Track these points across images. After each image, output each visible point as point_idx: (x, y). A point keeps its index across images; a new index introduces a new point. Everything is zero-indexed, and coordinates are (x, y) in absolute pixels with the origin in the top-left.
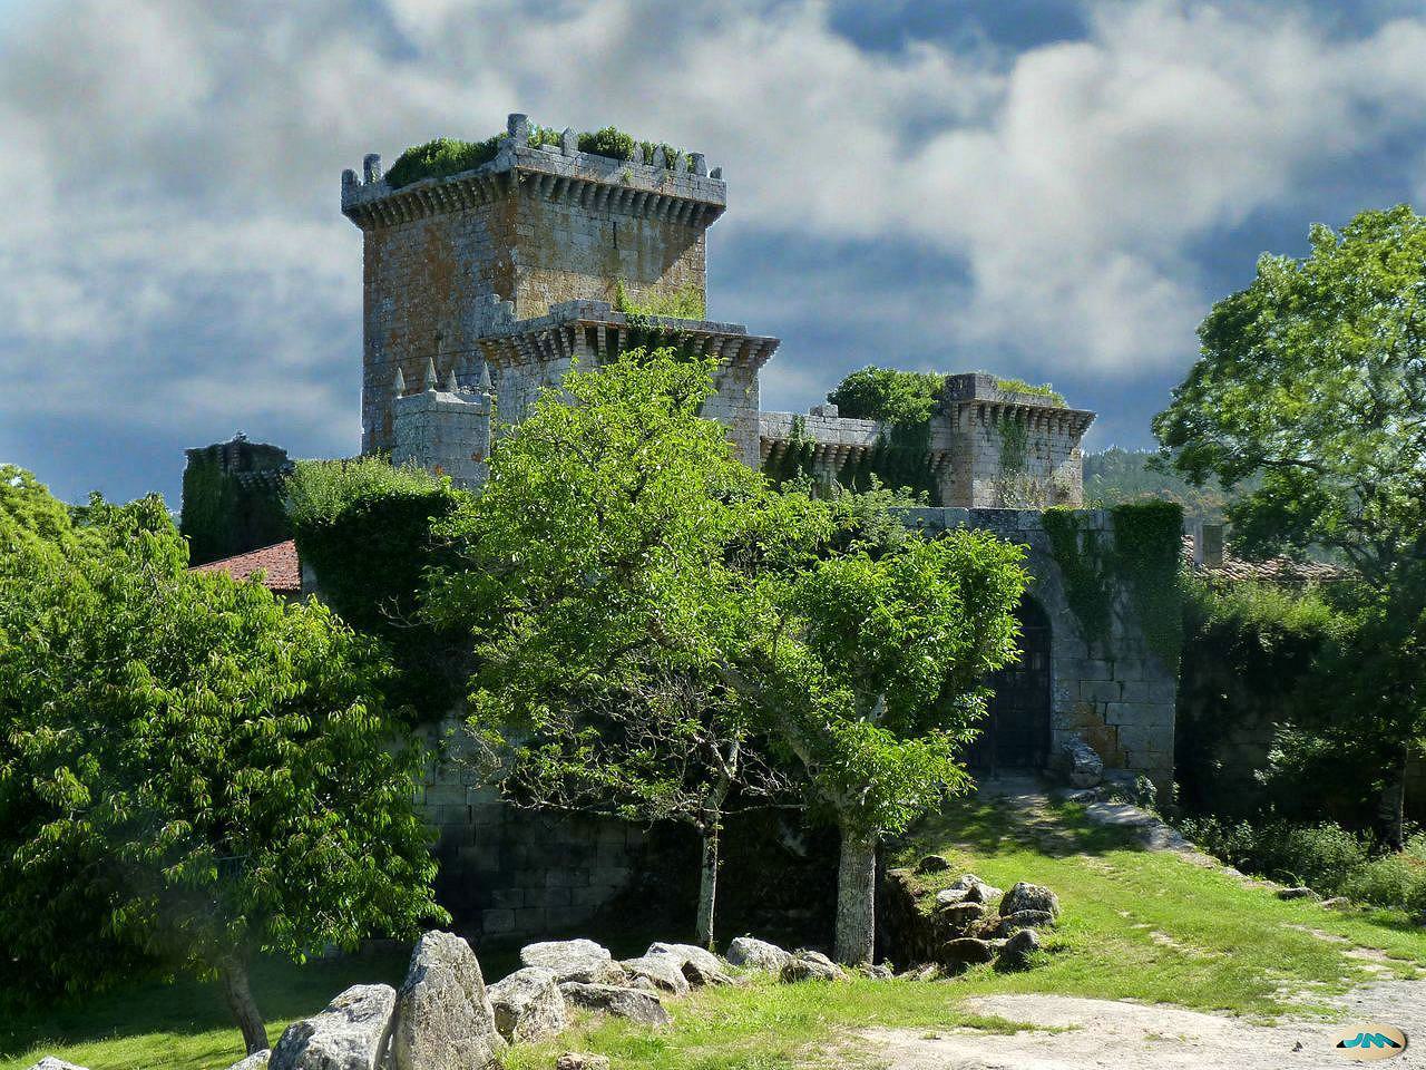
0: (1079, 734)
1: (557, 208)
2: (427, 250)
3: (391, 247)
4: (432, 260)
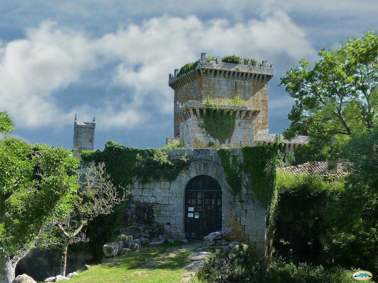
0: (231, 228)
1: (216, 79)
3: (179, 94)
4: (187, 96)
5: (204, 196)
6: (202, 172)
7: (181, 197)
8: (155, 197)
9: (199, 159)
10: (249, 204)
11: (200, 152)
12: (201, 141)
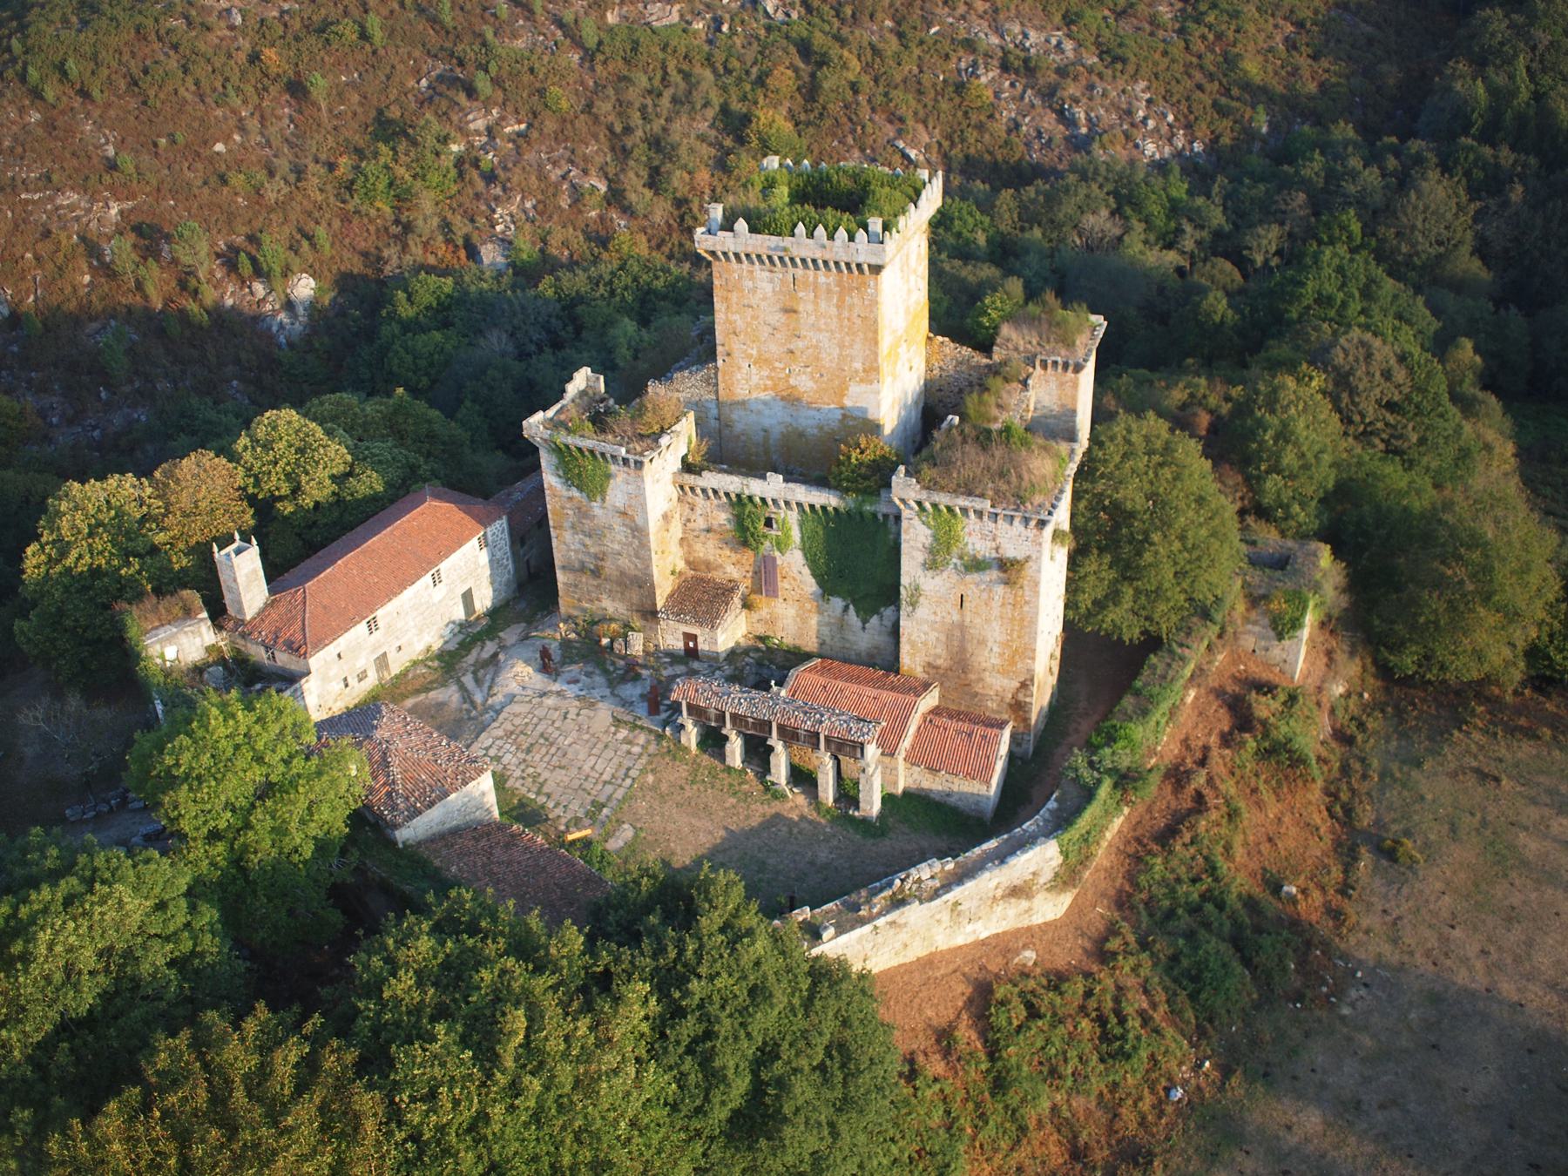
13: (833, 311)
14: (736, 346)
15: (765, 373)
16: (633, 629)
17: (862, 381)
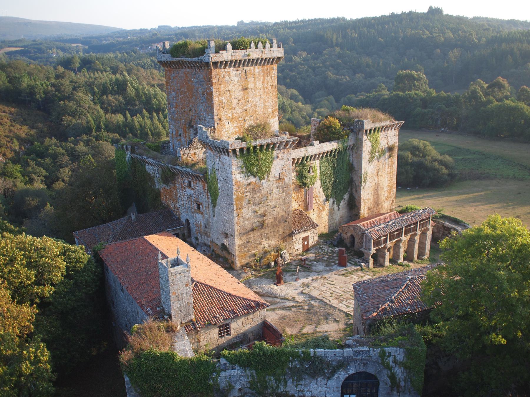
2: (185, 80)
4: (187, 83)
5: (359, 385)
6: (362, 369)
7: (338, 391)
8: (311, 392)
9: (359, 359)
10: (406, 393)
11: (359, 353)
12: (241, 182)
13: (261, 85)
14: (223, 114)
15: (235, 125)
16: (281, 250)
17: (272, 117)
